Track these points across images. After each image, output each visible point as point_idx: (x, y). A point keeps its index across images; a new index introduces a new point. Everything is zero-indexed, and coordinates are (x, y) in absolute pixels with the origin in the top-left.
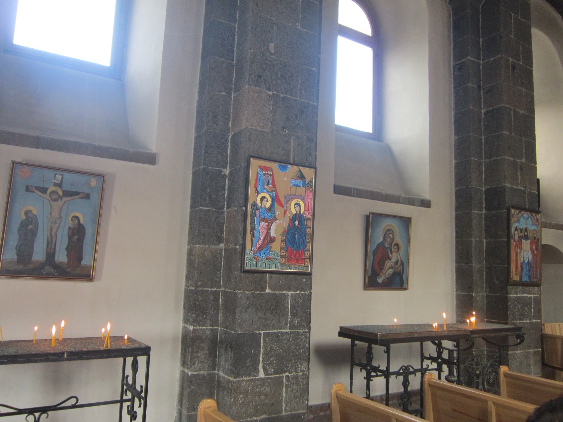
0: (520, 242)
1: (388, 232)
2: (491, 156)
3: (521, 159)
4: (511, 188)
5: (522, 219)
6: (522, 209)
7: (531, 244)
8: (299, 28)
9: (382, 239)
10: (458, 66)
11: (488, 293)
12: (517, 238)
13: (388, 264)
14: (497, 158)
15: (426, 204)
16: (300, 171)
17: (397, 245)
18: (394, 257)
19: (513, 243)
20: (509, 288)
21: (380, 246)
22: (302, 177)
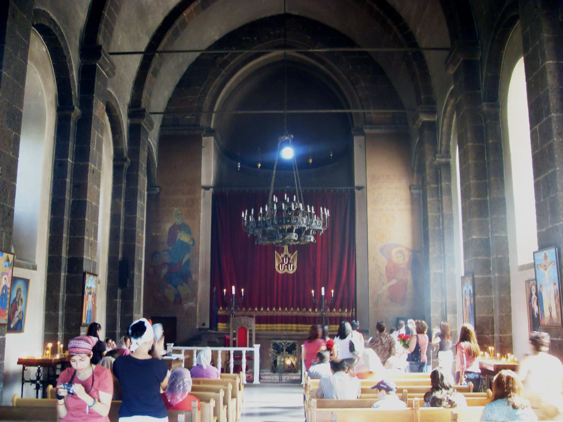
0: (88, 296)
1: (19, 290)
2: (75, 235)
3: (91, 238)
4: (86, 259)
5: (90, 280)
6: (90, 274)
7: (93, 297)
8: (11, 155)
9: (15, 296)
10: (58, 163)
11: (66, 333)
12: (87, 294)
13: (17, 313)
14: (80, 237)
15: (35, 268)
16: (8, 256)
17: (21, 299)
18: (20, 308)
19: (85, 297)
20: (81, 328)
21: (15, 300)
22: (8, 260)
